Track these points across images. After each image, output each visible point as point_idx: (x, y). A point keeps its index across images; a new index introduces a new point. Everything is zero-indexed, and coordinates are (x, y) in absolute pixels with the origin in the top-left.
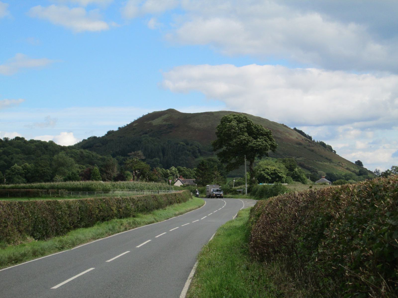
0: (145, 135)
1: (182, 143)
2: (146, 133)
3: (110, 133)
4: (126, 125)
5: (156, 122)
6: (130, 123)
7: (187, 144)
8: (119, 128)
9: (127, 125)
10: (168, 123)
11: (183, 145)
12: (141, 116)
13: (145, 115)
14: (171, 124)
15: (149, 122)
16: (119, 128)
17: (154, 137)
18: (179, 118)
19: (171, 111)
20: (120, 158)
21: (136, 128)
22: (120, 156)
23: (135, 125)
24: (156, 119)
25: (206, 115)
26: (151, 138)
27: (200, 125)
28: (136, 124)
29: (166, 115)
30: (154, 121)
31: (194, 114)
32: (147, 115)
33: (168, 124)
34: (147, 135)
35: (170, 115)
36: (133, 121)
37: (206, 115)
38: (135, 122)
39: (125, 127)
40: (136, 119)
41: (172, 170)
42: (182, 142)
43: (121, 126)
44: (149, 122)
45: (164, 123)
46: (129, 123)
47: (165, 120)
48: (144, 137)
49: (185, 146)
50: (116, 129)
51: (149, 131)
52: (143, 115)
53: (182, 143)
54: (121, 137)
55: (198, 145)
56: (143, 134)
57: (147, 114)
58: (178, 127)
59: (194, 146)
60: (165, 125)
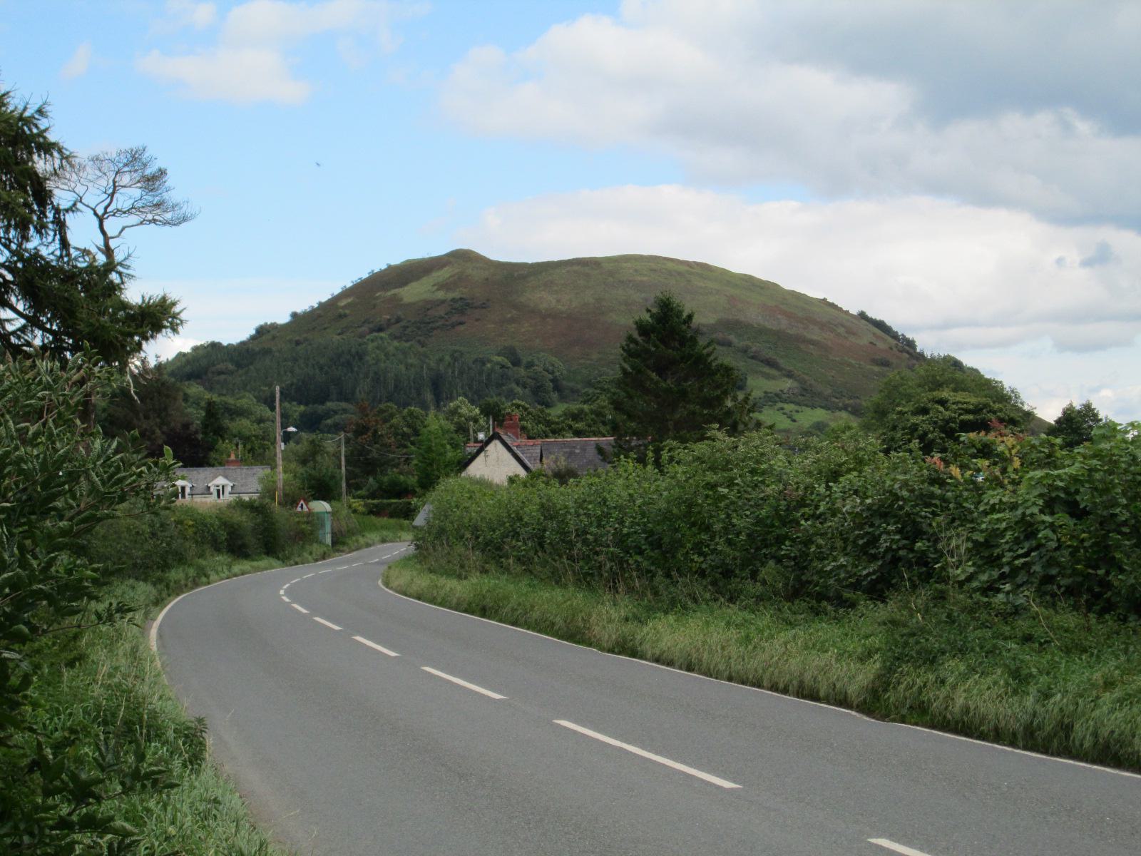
0: (376, 334)
1: (499, 359)
2: (380, 330)
3: (262, 331)
4: (316, 306)
5: (413, 293)
6: (330, 297)
7: (516, 363)
8: (294, 315)
9: (321, 304)
10: (451, 295)
11: (503, 367)
12: (365, 276)
13: (377, 270)
14: (461, 299)
15: (389, 294)
16: (294, 315)
17: (407, 341)
18: (487, 279)
19: (462, 257)
20: (294, 409)
21: (347, 312)
22: (295, 403)
23: (343, 303)
24: (414, 284)
25: (575, 268)
26: (396, 343)
27: (558, 301)
28: (350, 300)
29: (447, 268)
30: (406, 288)
31: (538, 265)
32: (385, 270)
33: (453, 300)
34: (382, 334)
35: (456, 271)
36: (337, 291)
37: (575, 268)
38: (346, 293)
39: (313, 311)
40: (349, 285)
41: (460, 416)
42: (499, 355)
43: (299, 310)
44: (389, 294)
45: (441, 295)
46: (324, 299)
47: (442, 286)
48: (372, 341)
49: (508, 368)
50: (283, 318)
51: (389, 320)
52: (370, 271)
53: (499, 359)
54: (298, 343)
55: (553, 365)
56: (372, 331)
57: (384, 267)
58: (485, 308)
59: (540, 369)
60: (443, 302)
